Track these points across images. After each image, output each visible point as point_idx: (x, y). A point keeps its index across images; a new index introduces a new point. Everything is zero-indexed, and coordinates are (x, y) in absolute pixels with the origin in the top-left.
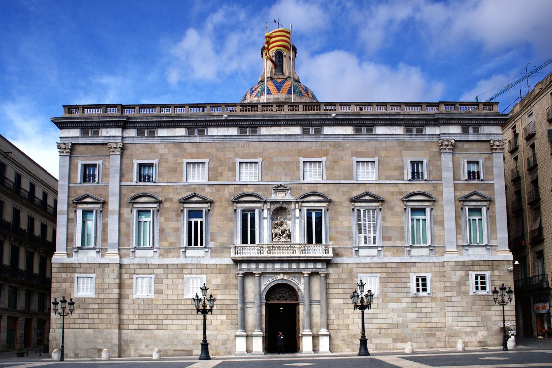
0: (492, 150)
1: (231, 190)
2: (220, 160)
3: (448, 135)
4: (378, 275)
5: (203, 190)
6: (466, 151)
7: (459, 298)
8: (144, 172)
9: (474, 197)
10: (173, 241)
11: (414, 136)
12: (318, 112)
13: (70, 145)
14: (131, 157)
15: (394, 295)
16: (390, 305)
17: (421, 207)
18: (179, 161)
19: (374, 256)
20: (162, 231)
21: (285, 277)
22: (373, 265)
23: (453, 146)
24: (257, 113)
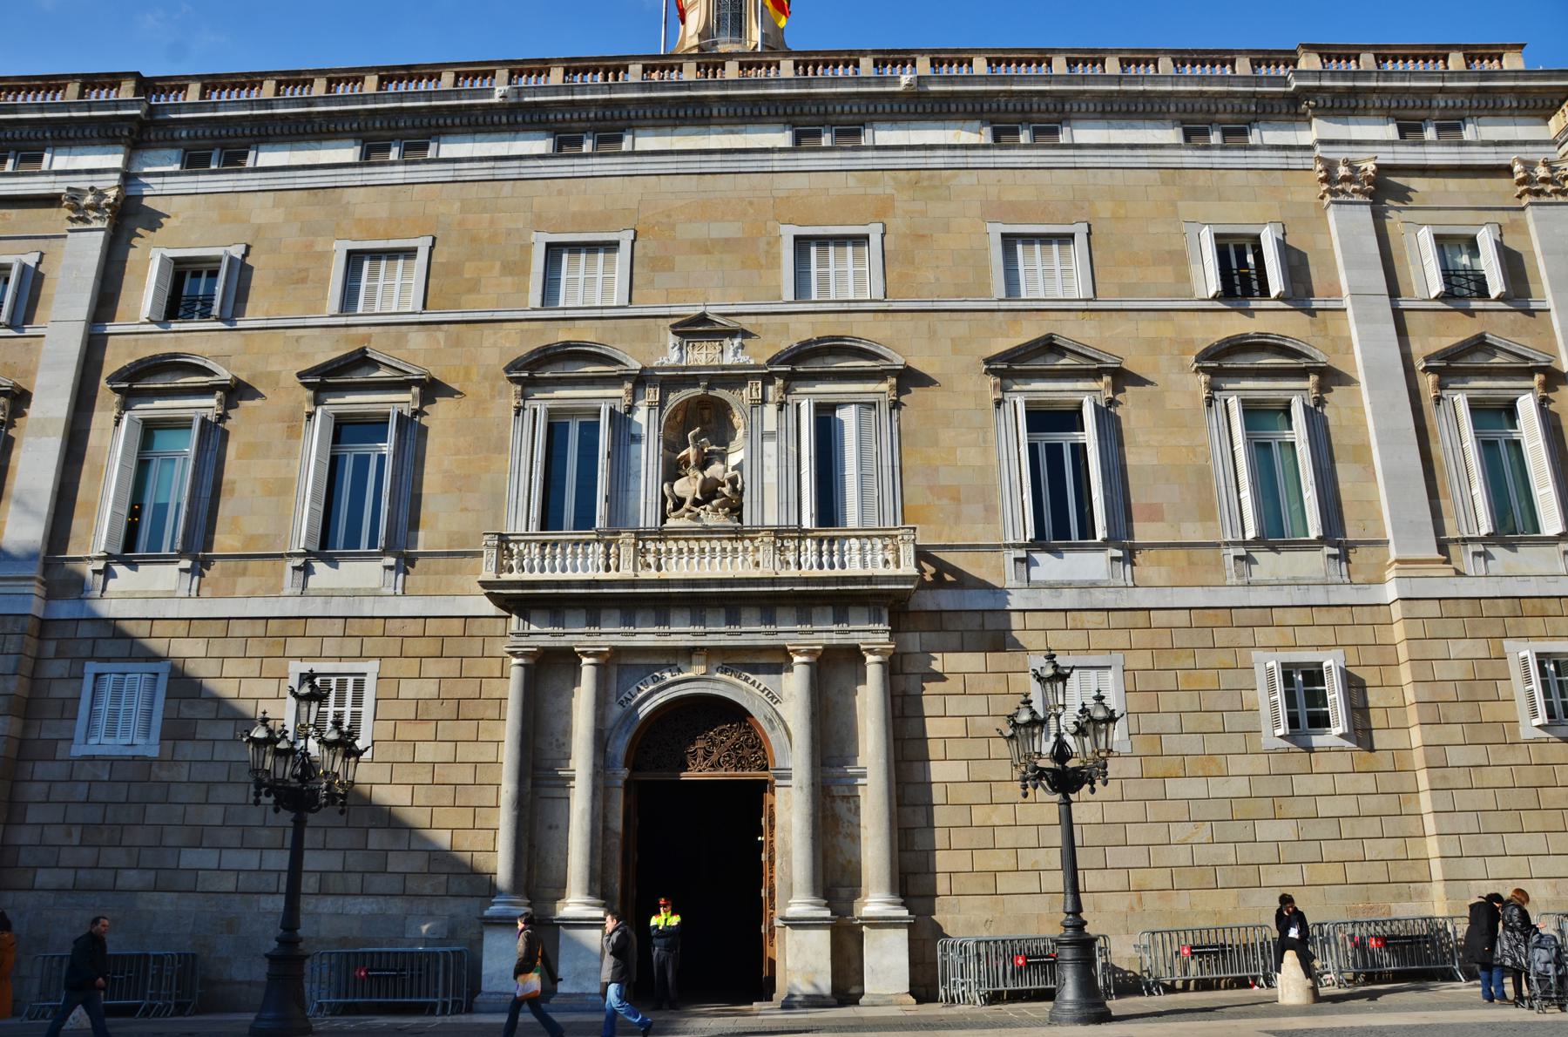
2: (474, 239)
7: (1476, 755)
10: (261, 531)
15: (1192, 744)
16: (1175, 787)
18: (319, 248)
19: (1094, 585)
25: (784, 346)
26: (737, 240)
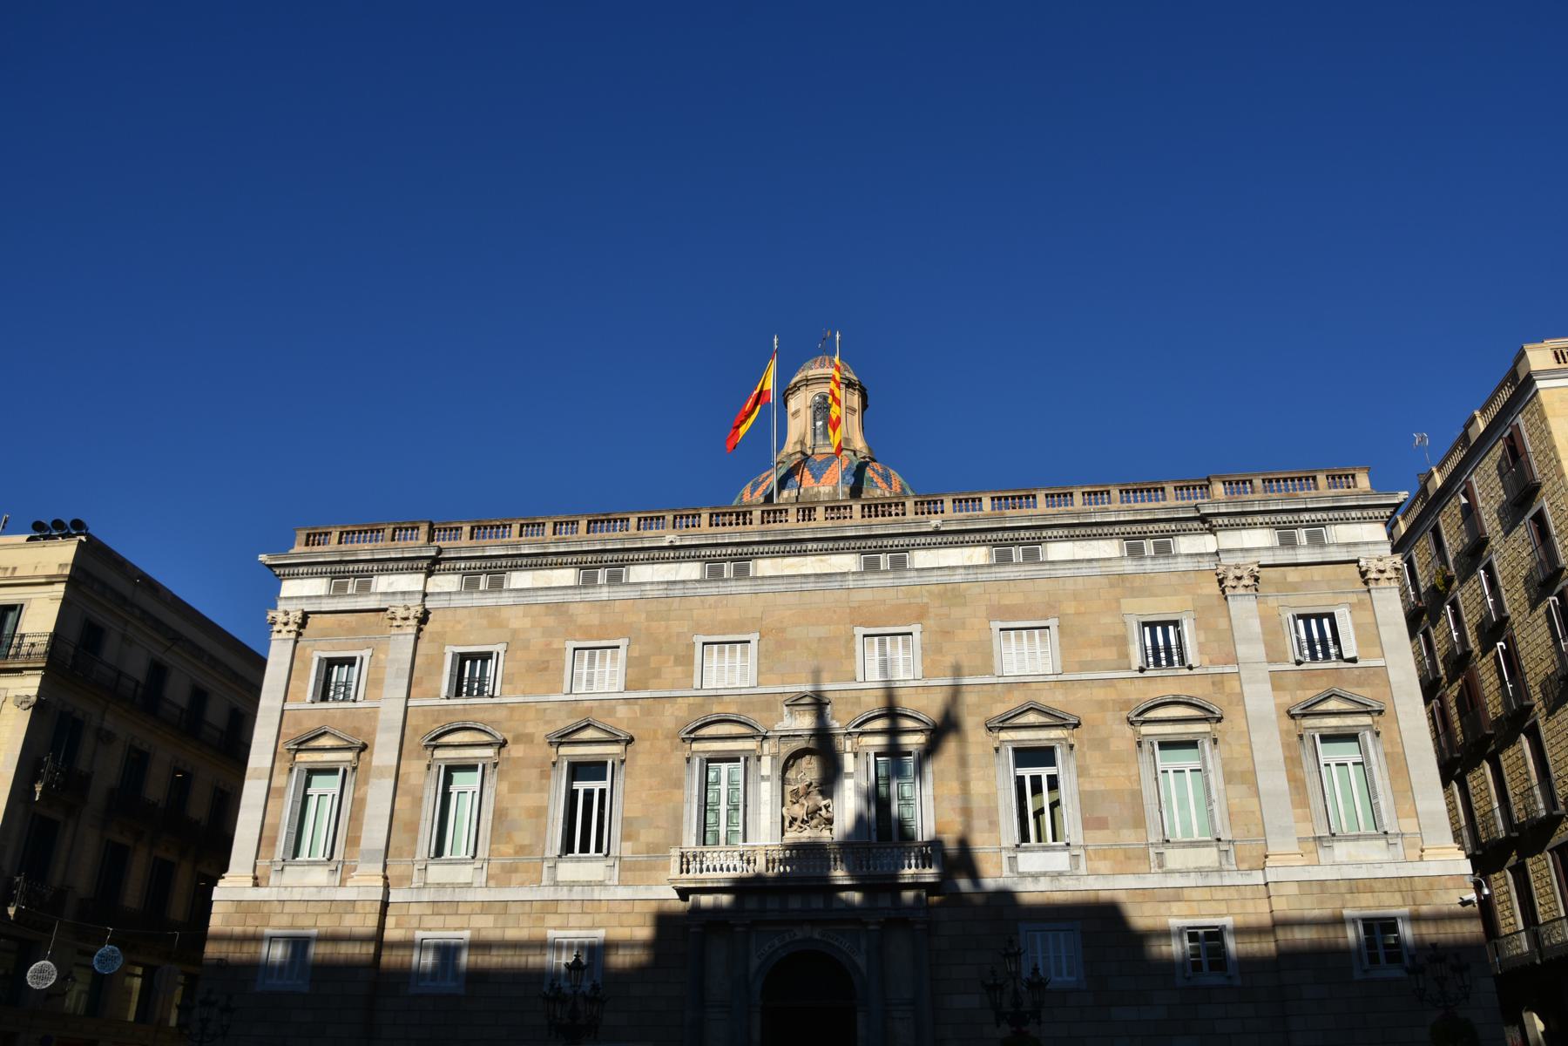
5: (611, 712)
6: (1295, 588)
8: (469, 672)
9: (1332, 705)
10: (526, 842)
13: (299, 614)
14: (441, 640)
19: (1060, 874)
23: (1257, 579)
25: (858, 712)
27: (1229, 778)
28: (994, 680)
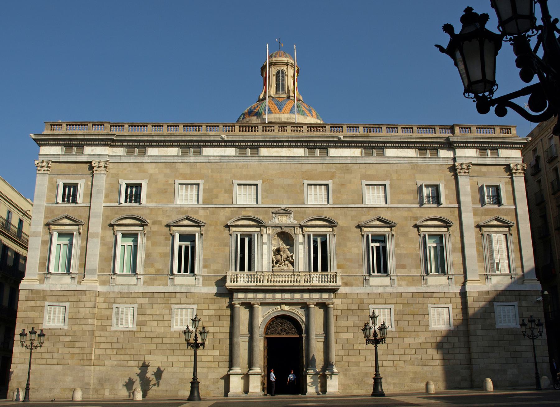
0: (511, 175)
1: (227, 213)
3: (464, 159)
4: (392, 306)
5: (196, 213)
6: (484, 175)
9: (495, 223)
10: (160, 268)
11: (427, 159)
12: (324, 133)
14: (116, 177)
16: (407, 340)
17: (438, 233)
18: (170, 182)
19: (387, 286)
20: (148, 256)
21: (286, 308)
22: (385, 295)
24: (257, 134)
26: (291, 184)
27: (454, 251)
28: (362, 206)
